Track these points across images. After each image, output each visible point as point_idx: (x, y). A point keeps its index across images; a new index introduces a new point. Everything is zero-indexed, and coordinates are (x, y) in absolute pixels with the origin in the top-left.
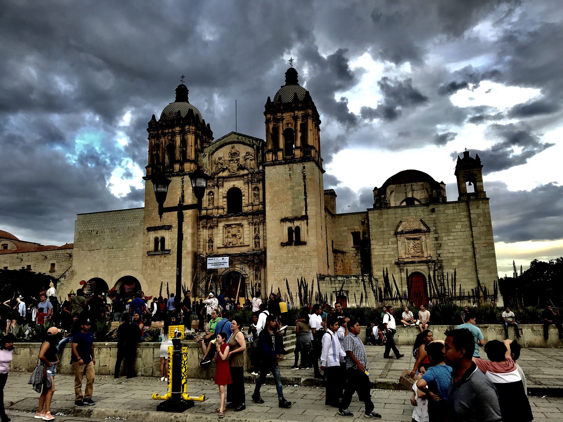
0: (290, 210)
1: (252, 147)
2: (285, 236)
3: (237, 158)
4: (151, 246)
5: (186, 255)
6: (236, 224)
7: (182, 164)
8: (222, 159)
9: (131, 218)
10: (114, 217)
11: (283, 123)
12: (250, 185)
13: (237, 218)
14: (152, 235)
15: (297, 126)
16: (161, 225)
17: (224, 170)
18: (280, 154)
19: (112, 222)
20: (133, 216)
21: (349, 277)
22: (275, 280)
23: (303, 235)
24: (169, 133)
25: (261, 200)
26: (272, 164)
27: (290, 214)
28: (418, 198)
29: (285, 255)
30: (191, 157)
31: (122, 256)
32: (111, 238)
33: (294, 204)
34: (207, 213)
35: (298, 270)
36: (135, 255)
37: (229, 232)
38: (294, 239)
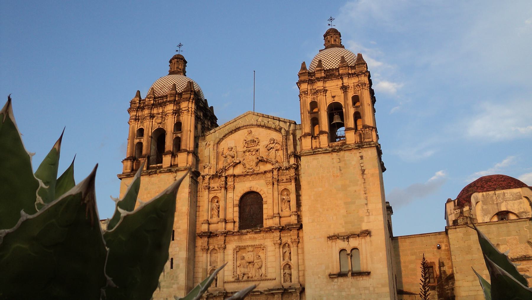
1: (279, 130)
2: (335, 263)
3: (255, 148)
6: (254, 245)
7: (174, 155)
8: (233, 150)
11: (326, 96)
12: (275, 186)
13: (256, 236)
15: (347, 100)
17: (236, 165)
18: (324, 140)
23: (365, 261)
24: (158, 114)
25: (294, 208)
28: (516, 212)
30: (188, 146)
34: (209, 229)
37: (243, 258)
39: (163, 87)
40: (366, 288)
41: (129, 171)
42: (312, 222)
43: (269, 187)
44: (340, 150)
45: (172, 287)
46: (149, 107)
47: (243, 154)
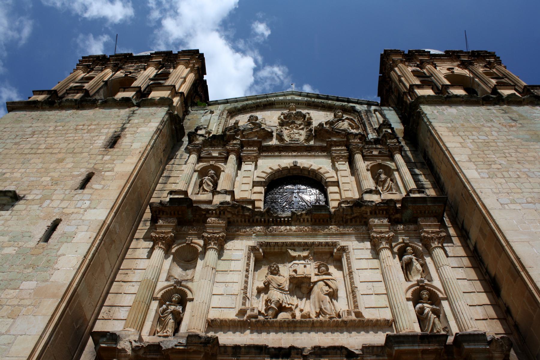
12: (358, 157)
43: (339, 163)
47: (279, 127)
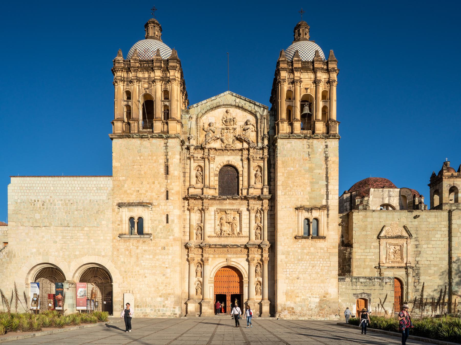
0: (307, 196)
4: (124, 226)
5: (173, 242)
9: (95, 189)
10: (68, 185)
14: (126, 213)
16: (138, 201)
19: (65, 191)
20: (96, 186)
21: (373, 279)
22: (286, 279)
23: (322, 228)
24: (145, 78)
26: (287, 136)
27: (308, 201)
29: (299, 251)
30: (176, 116)
31: (83, 237)
32: (66, 213)
33: (312, 190)
35: (314, 268)
36: (102, 238)
38: (311, 233)
39: (147, 50)
40: (321, 248)
41: (120, 132)
42: (284, 195)
44: (310, 138)
45: (168, 238)
46: (135, 69)
